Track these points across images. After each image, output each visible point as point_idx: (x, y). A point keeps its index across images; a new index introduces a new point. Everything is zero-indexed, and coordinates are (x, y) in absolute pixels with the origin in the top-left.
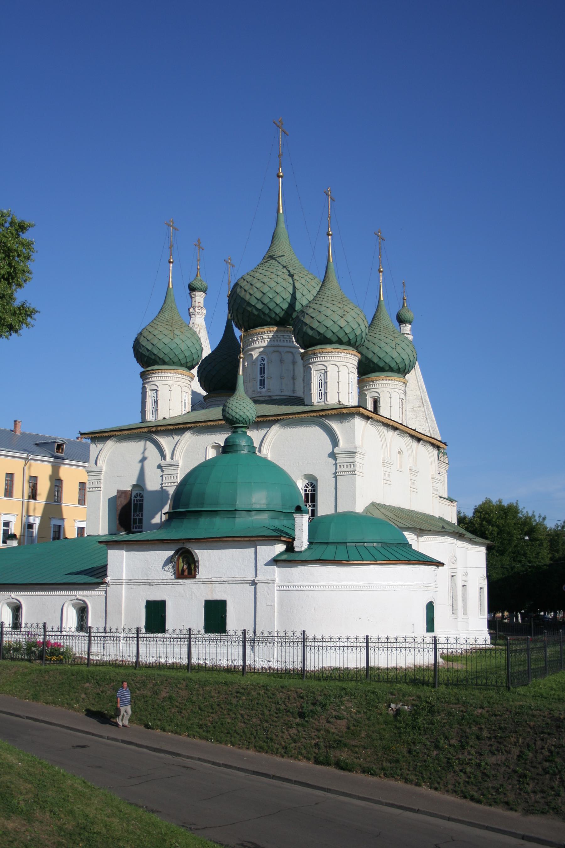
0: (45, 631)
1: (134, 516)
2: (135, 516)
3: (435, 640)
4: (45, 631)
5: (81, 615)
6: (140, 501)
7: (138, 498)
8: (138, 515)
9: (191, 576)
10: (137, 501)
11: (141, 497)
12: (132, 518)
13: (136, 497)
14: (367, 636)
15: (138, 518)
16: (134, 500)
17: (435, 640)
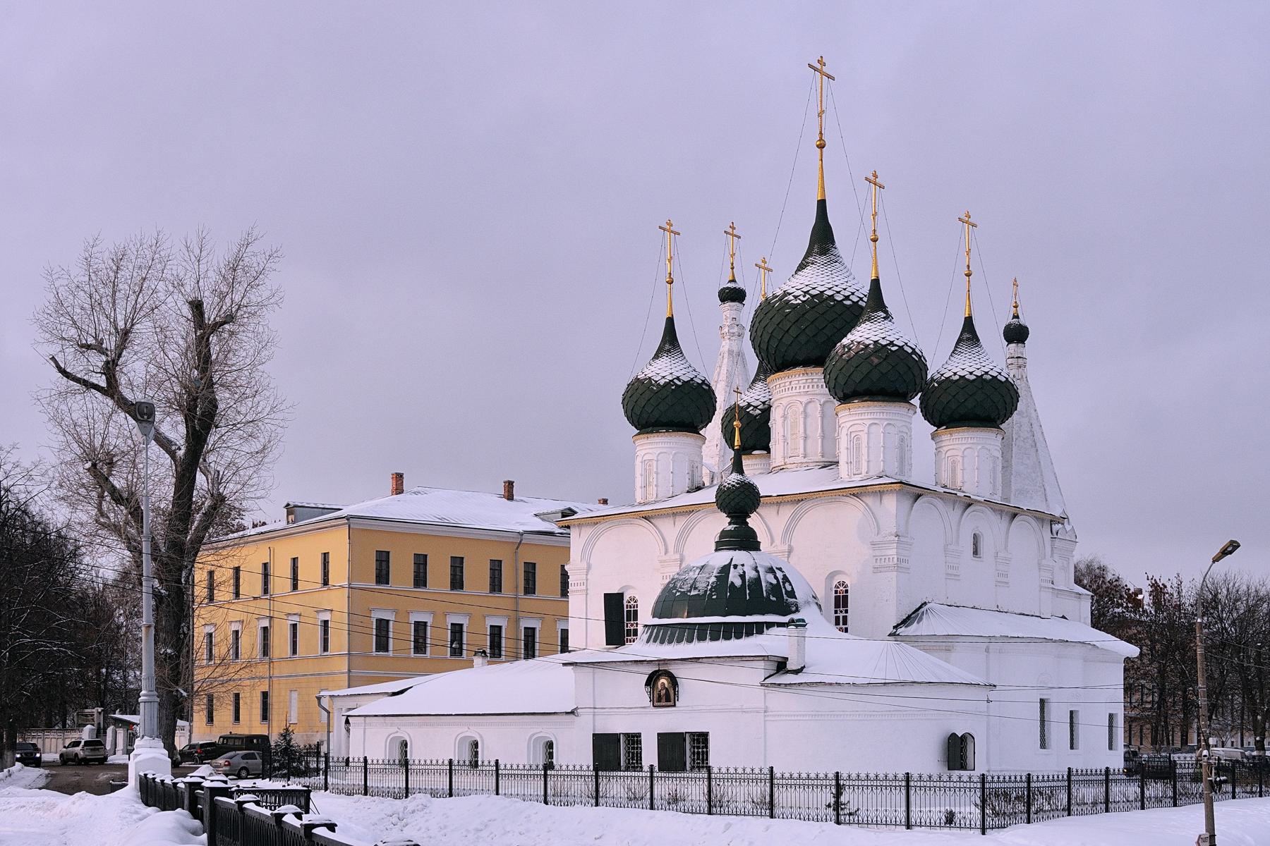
0: (497, 770)
1: (627, 627)
2: (629, 625)
3: (908, 778)
4: (497, 770)
5: (548, 751)
6: (634, 607)
7: (632, 603)
8: (632, 625)
9: (669, 703)
10: (631, 607)
11: (635, 602)
12: (626, 628)
13: (629, 602)
14: (837, 773)
15: (632, 628)
16: (627, 605)
17: (908, 778)
